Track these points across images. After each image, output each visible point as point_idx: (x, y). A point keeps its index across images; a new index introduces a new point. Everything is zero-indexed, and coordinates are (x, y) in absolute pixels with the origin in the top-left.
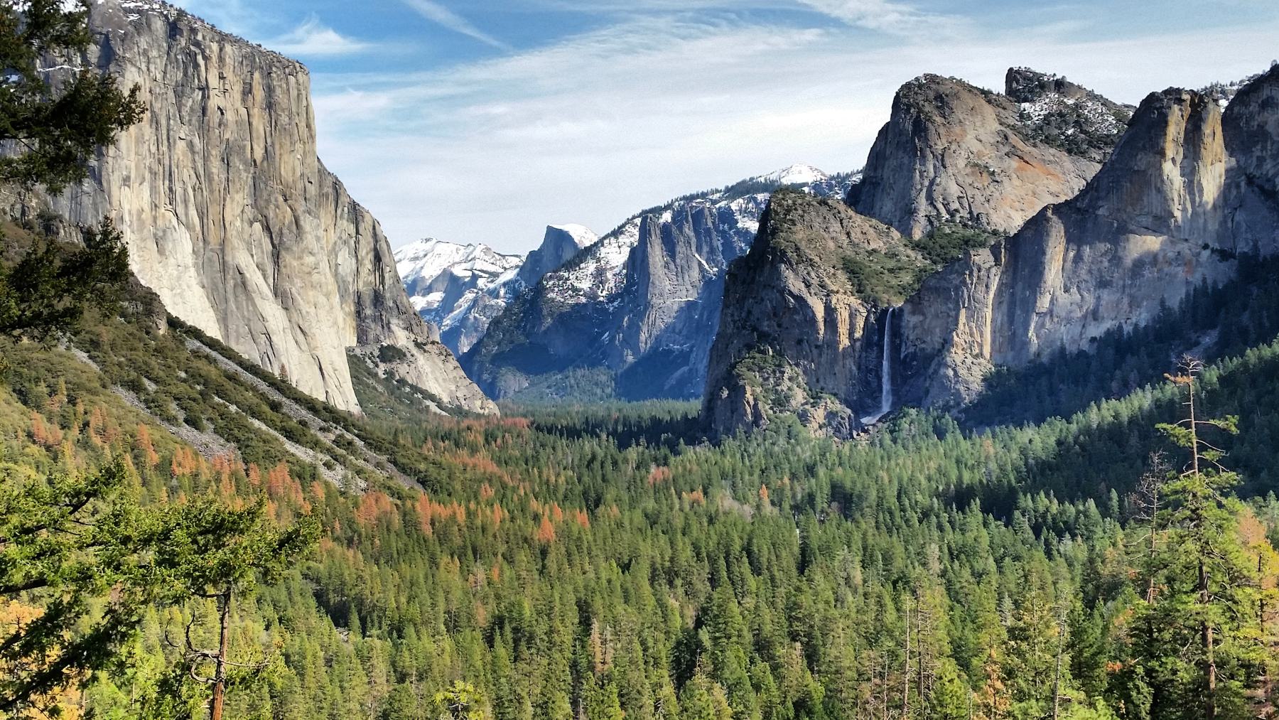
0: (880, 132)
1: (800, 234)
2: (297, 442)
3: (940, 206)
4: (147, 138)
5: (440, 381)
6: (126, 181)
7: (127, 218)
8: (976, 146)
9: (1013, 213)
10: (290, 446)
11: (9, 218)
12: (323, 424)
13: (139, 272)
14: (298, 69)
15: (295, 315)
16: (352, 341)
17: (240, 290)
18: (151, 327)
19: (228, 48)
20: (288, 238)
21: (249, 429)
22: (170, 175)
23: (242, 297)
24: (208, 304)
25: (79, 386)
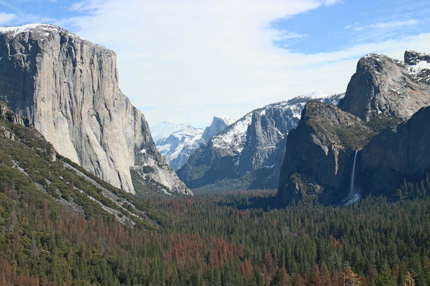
0: (352, 77)
1: (319, 120)
2: (107, 206)
3: (377, 108)
4: (51, 82)
5: (169, 181)
6: (43, 100)
8: (392, 83)
9: (408, 111)
10: (103, 207)
12: (118, 198)
13: (47, 136)
14: (112, 53)
15: (109, 153)
17: (87, 143)
18: (49, 158)
19: (85, 46)
20: (107, 121)
21: (88, 200)
22: (60, 97)
23: (88, 146)
24: (74, 149)
25: (20, 182)
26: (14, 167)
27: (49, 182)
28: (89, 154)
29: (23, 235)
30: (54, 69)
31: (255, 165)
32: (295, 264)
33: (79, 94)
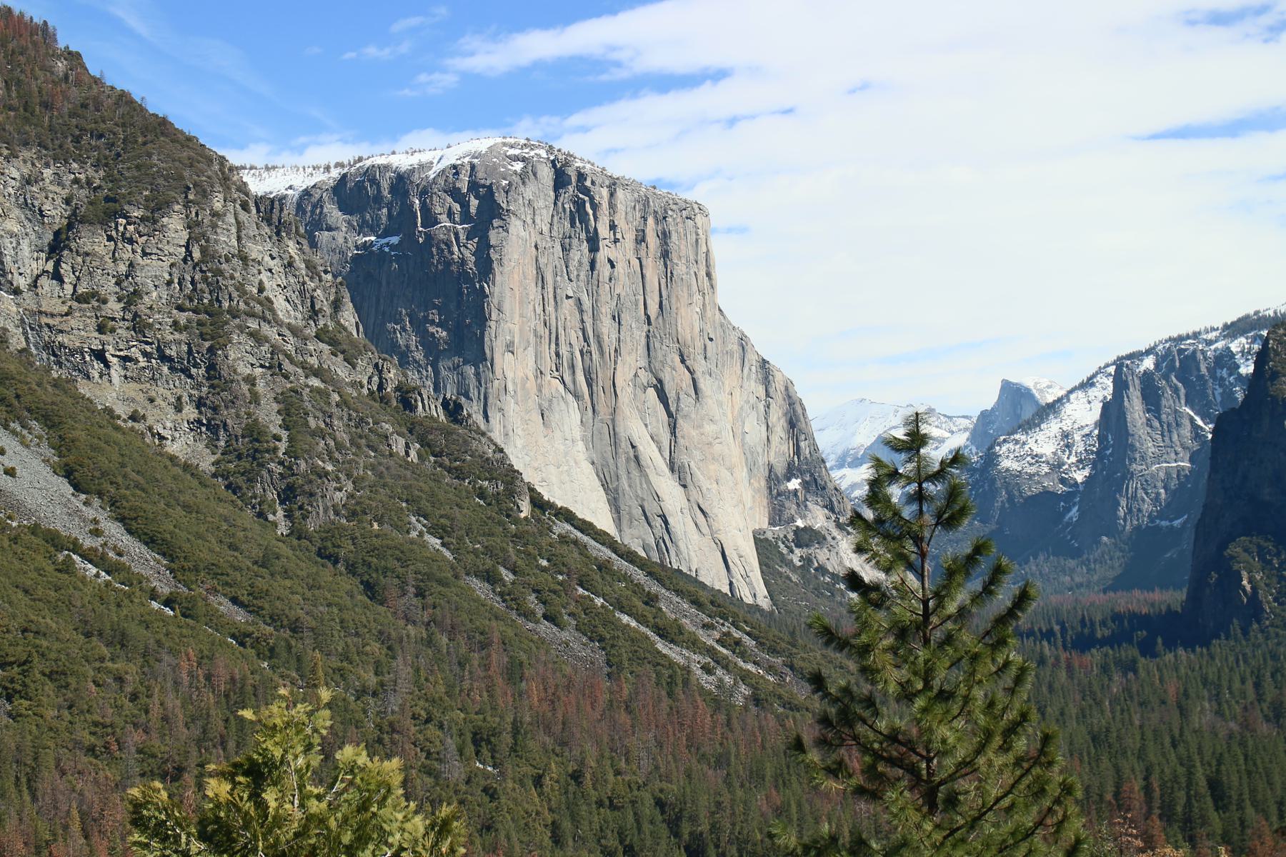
2: (672, 641)
4: (532, 297)
6: (510, 348)
7: (510, 387)
10: (661, 646)
11: (365, 391)
12: (707, 620)
13: (524, 447)
14: (697, 211)
16: (761, 521)
17: (633, 464)
18: (512, 509)
19: (620, 194)
20: (687, 402)
21: (617, 625)
22: (557, 338)
23: (635, 473)
24: (599, 484)
25: (429, 576)
26: (414, 534)
27: (508, 576)
28: (637, 496)
29: (428, 721)
30: (537, 260)
31: (1125, 520)
32: (1214, 816)
33: (607, 326)
